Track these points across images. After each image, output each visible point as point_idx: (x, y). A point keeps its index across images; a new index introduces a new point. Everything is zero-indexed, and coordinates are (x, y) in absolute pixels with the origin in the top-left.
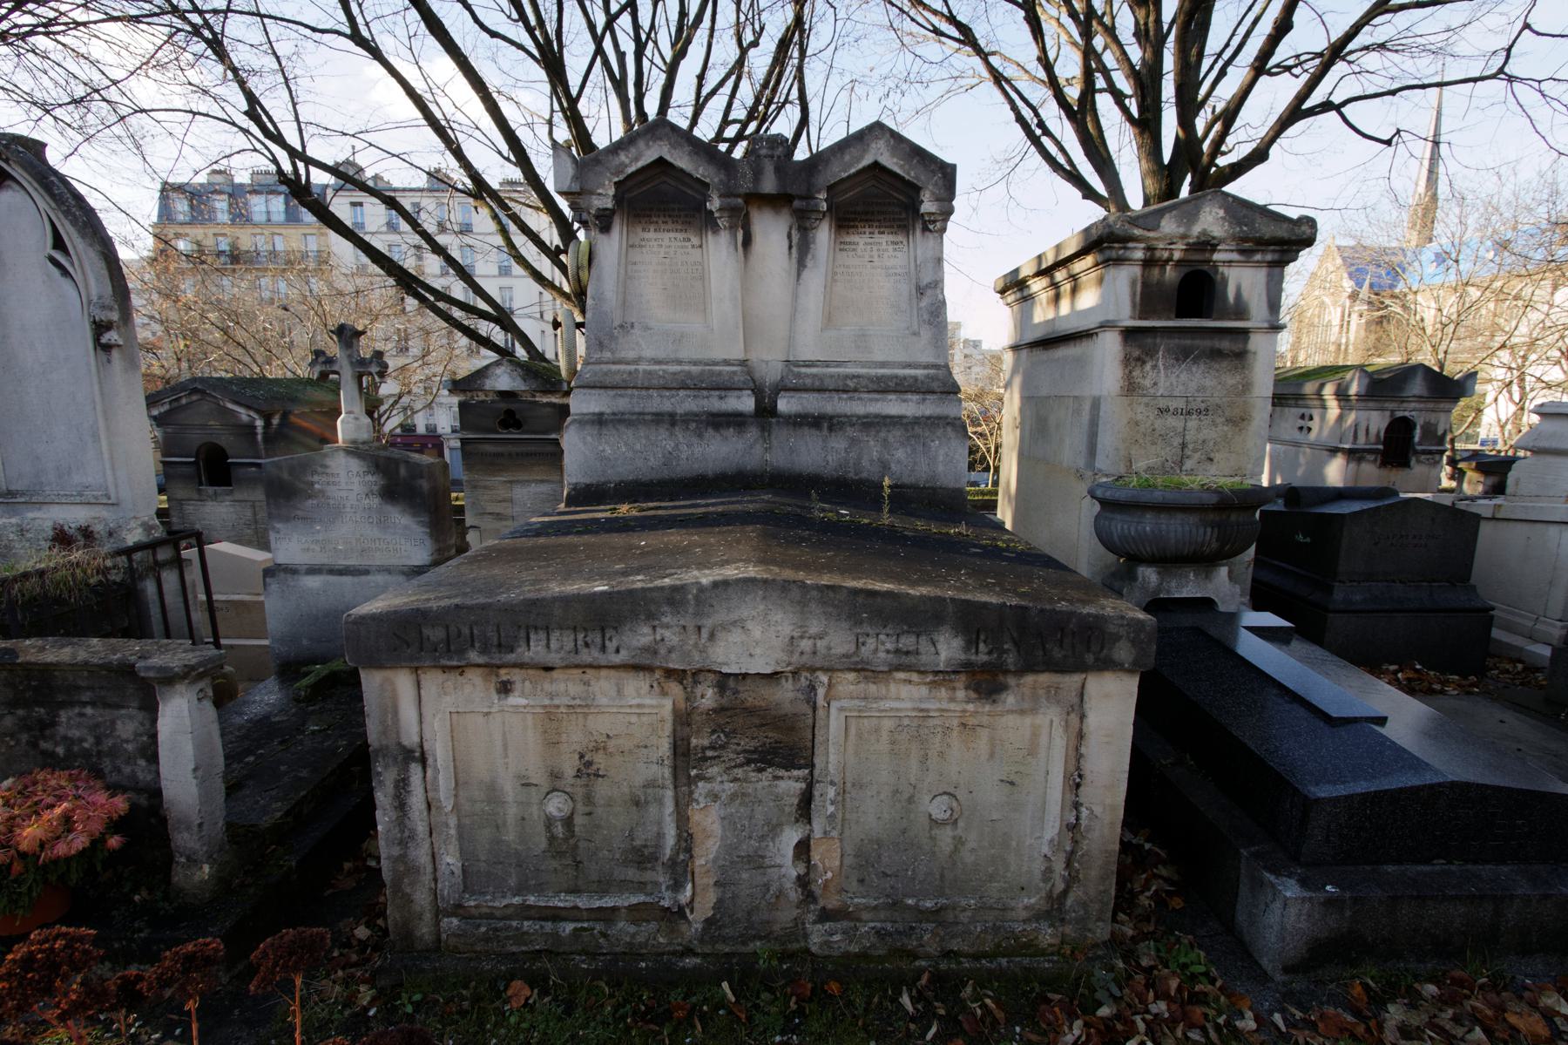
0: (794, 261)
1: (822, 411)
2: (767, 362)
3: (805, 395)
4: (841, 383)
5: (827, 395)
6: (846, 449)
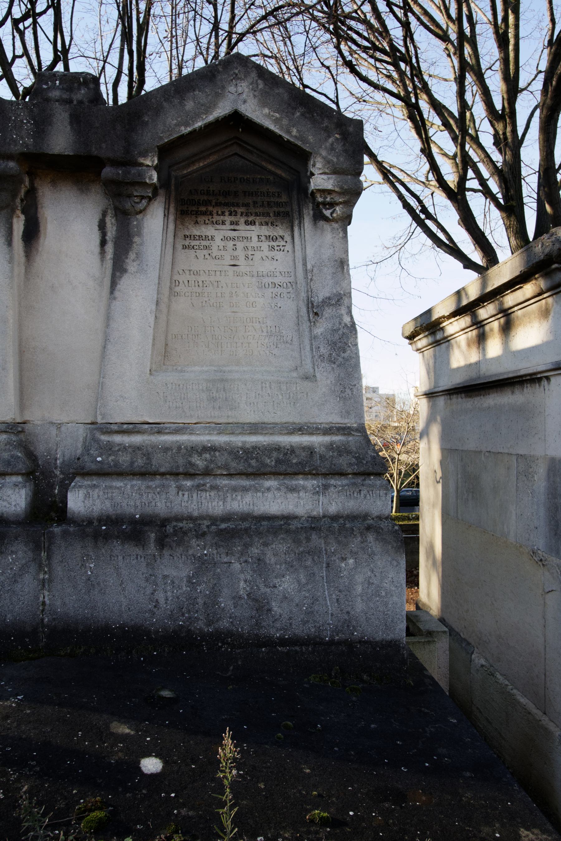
0: (109, 264)
1: (149, 510)
2: (59, 426)
3: (118, 483)
4: (181, 461)
5: (158, 481)
6: (189, 580)
